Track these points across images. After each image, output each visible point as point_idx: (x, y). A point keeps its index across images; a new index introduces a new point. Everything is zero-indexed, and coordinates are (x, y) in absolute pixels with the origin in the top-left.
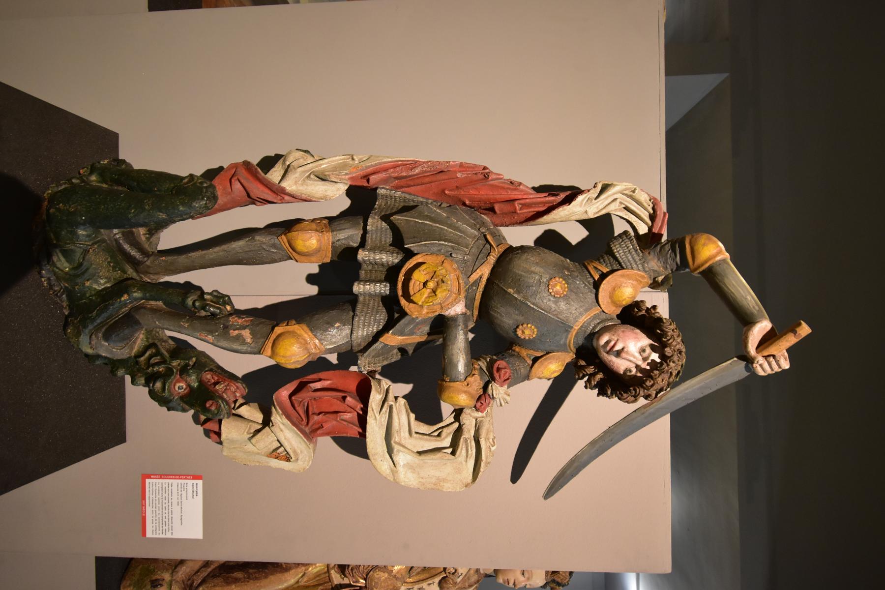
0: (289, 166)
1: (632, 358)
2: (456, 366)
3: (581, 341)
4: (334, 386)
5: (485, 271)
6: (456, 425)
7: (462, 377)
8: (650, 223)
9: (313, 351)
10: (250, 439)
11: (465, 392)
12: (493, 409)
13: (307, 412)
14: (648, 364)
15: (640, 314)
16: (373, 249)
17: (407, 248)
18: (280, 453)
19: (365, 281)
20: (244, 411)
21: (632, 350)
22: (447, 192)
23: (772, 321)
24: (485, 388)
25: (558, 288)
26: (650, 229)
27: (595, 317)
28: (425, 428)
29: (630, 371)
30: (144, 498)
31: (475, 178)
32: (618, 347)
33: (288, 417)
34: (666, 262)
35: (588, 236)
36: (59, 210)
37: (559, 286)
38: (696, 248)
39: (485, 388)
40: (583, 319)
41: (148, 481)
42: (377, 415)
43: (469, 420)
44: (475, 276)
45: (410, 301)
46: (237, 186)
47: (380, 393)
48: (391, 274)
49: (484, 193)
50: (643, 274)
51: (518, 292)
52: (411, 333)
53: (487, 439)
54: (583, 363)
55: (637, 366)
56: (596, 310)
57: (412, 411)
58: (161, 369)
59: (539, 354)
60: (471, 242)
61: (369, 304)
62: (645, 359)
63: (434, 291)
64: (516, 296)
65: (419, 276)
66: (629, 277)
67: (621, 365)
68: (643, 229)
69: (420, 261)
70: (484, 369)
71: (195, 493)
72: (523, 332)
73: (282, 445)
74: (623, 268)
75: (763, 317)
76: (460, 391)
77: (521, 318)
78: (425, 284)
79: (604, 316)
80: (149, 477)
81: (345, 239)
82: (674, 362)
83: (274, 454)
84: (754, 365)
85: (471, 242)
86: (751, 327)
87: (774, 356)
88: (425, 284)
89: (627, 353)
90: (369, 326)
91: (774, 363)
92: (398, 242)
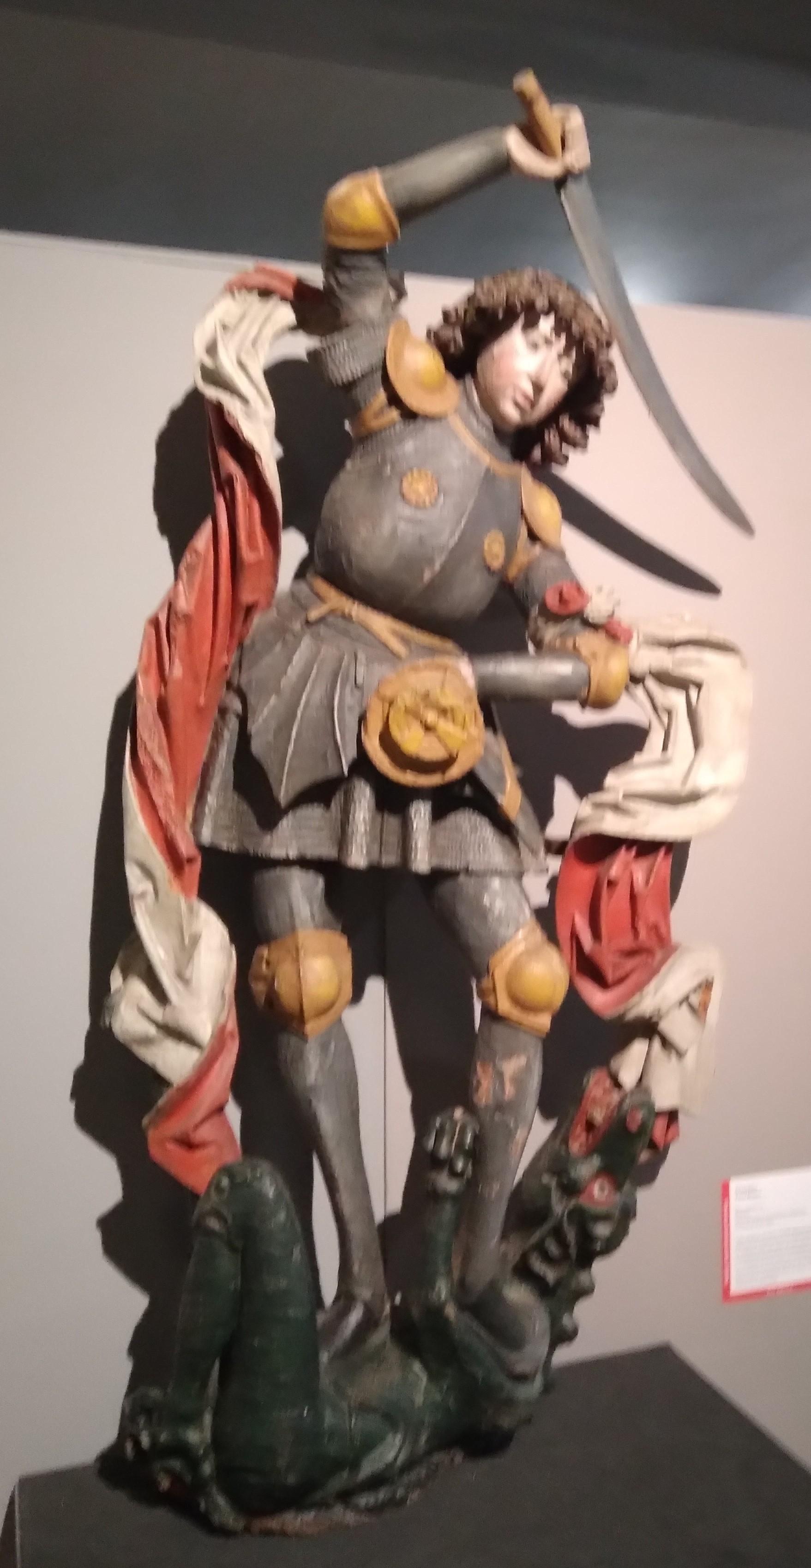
3: (506, 453)
4: (586, 910)
5: (381, 624)
6: (651, 683)
10: (680, 1055)
12: (625, 616)
13: (631, 953)
16: (342, 840)
17: (349, 771)
18: (697, 1004)
20: (628, 1076)
21: (530, 364)
24: (595, 627)
28: (655, 739)
32: (529, 389)
33: (640, 987)
37: (418, 487)
39: (595, 627)
43: (646, 659)
45: (450, 761)
47: (602, 819)
48: (392, 800)
56: (456, 423)
58: (565, 1242)
60: (328, 652)
63: (443, 712)
64: (437, 567)
65: (413, 740)
66: (399, 356)
67: (555, 387)
73: (686, 999)
78: (428, 728)
83: (699, 1012)
88: (428, 728)
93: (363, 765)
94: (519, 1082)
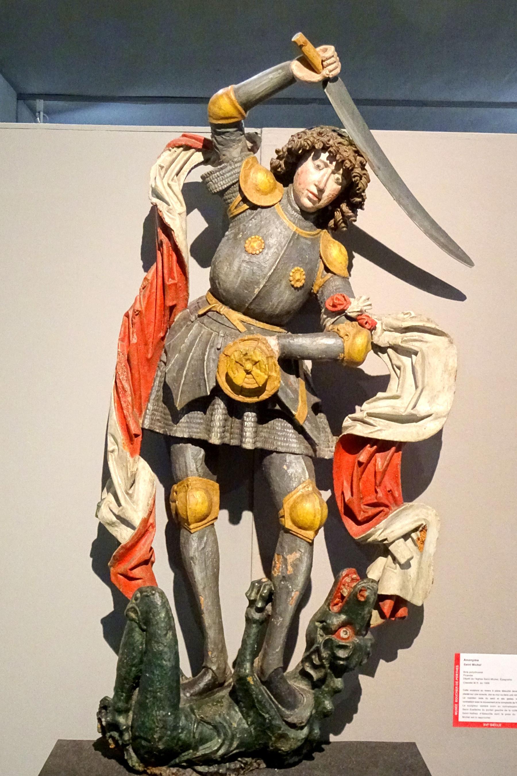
0: (118, 517)
1: (325, 179)
2: (328, 346)
3: (310, 224)
6: (390, 351)
7: (339, 341)
8: (192, 150)
9: (310, 489)
11: (354, 338)
12: (373, 313)
14: (331, 163)
15: (283, 166)
16: (209, 431)
19: (242, 436)
22: (149, 356)
23: (291, 59)
25: (255, 245)
26: (198, 150)
27: (285, 210)
29: (338, 179)
30: (480, 725)
31: (138, 324)
34: (233, 141)
35: (200, 210)
36: (160, 739)
37: (254, 244)
38: (222, 116)
40: (287, 222)
41: (461, 719)
42: (376, 429)
44: (241, 327)
46: (137, 572)
47: (355, 426)
48: (235, 410)
49: (153, 316)
50: (244, 162)
51: (258, 283)
52: (295, 392)
53: (403, 320)
54: (332, 223)
55: (333, 173)
57: (375, 395)
59: (322, 266)
60: (205, 330)
61: (265, 437)
62: (326, 166)
64: (261, 286)
66: (247, 176)
68: (199, 157)
69: (224, 378)
70: (333, 320)
71: (475, 663)
72: (298, 281)
74: (238, 181)
75: (288, 66)
76: (352, 344)
77: (284, 283)
78: (248, 372)
79: (285, 201)
80: (456, 717)
81: (196, 462)
82: (329, 141)
84: (331, 76)
85: (205, 330)
86: (296, 77)
87: (322, 61)
88: (248, 372)
89: (320, 182)
90: (287, 437)
91: (328, 62)
92: (201, 404)
93: (217, 391)
94: (295, 566)
